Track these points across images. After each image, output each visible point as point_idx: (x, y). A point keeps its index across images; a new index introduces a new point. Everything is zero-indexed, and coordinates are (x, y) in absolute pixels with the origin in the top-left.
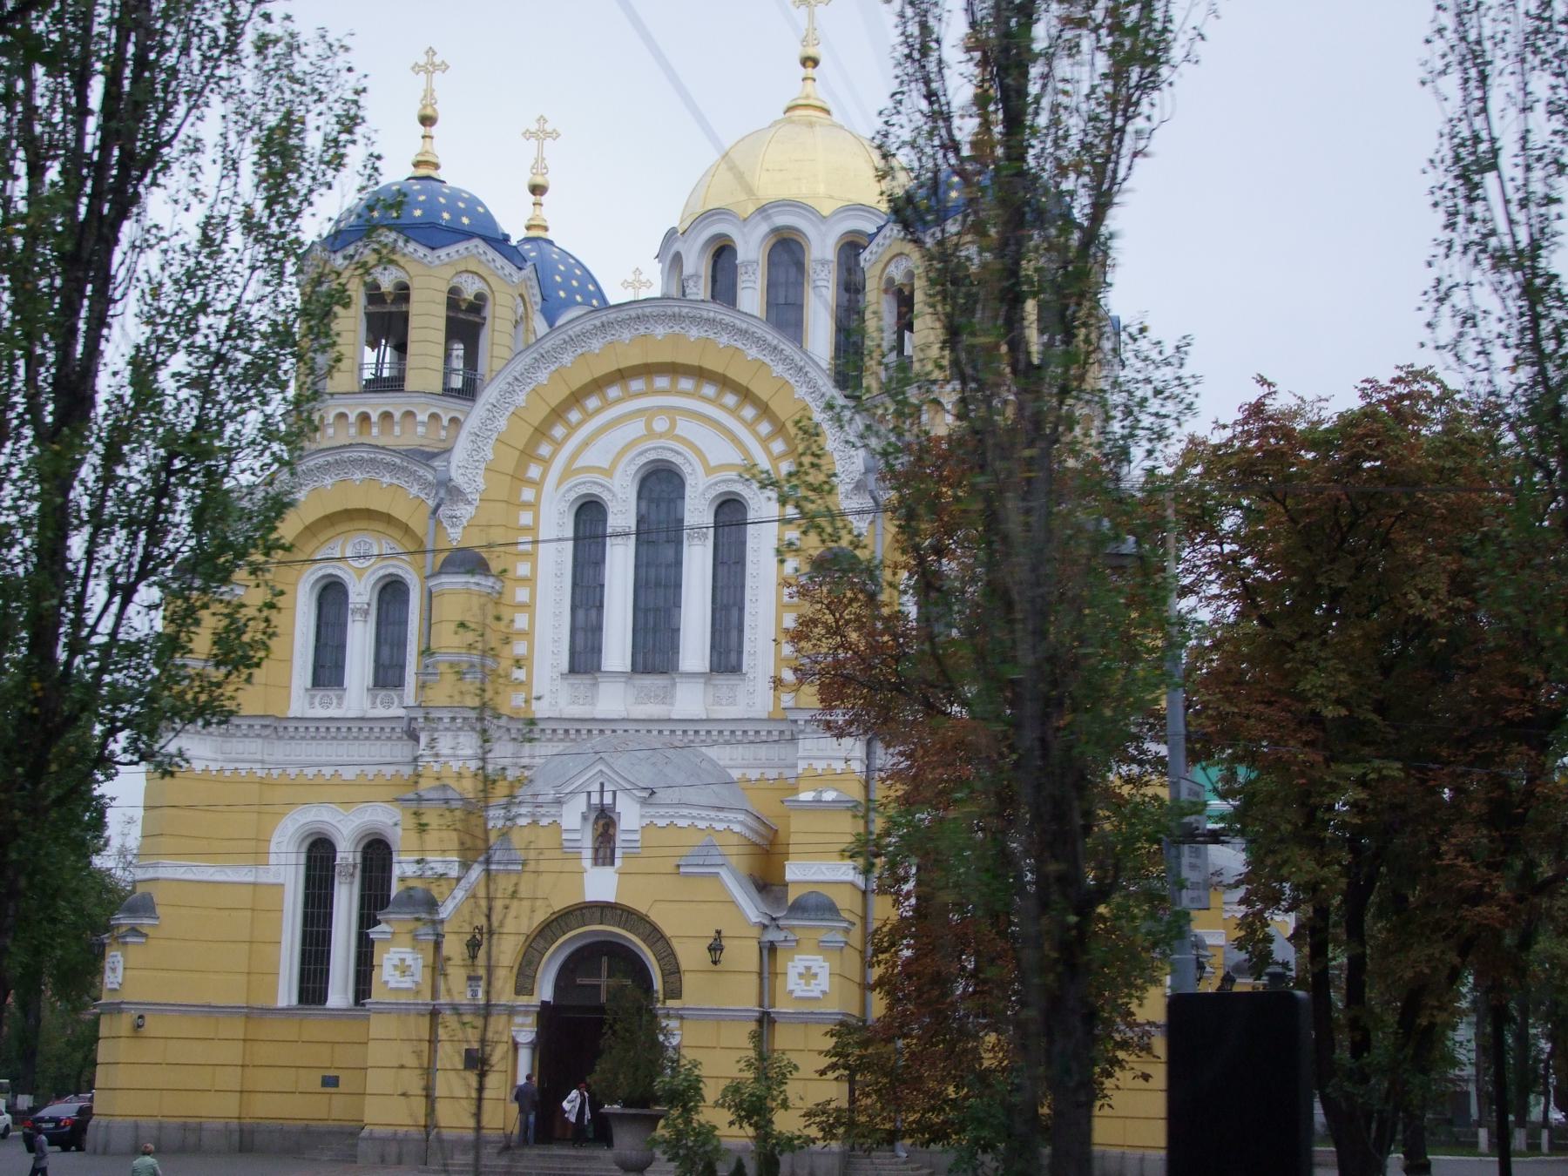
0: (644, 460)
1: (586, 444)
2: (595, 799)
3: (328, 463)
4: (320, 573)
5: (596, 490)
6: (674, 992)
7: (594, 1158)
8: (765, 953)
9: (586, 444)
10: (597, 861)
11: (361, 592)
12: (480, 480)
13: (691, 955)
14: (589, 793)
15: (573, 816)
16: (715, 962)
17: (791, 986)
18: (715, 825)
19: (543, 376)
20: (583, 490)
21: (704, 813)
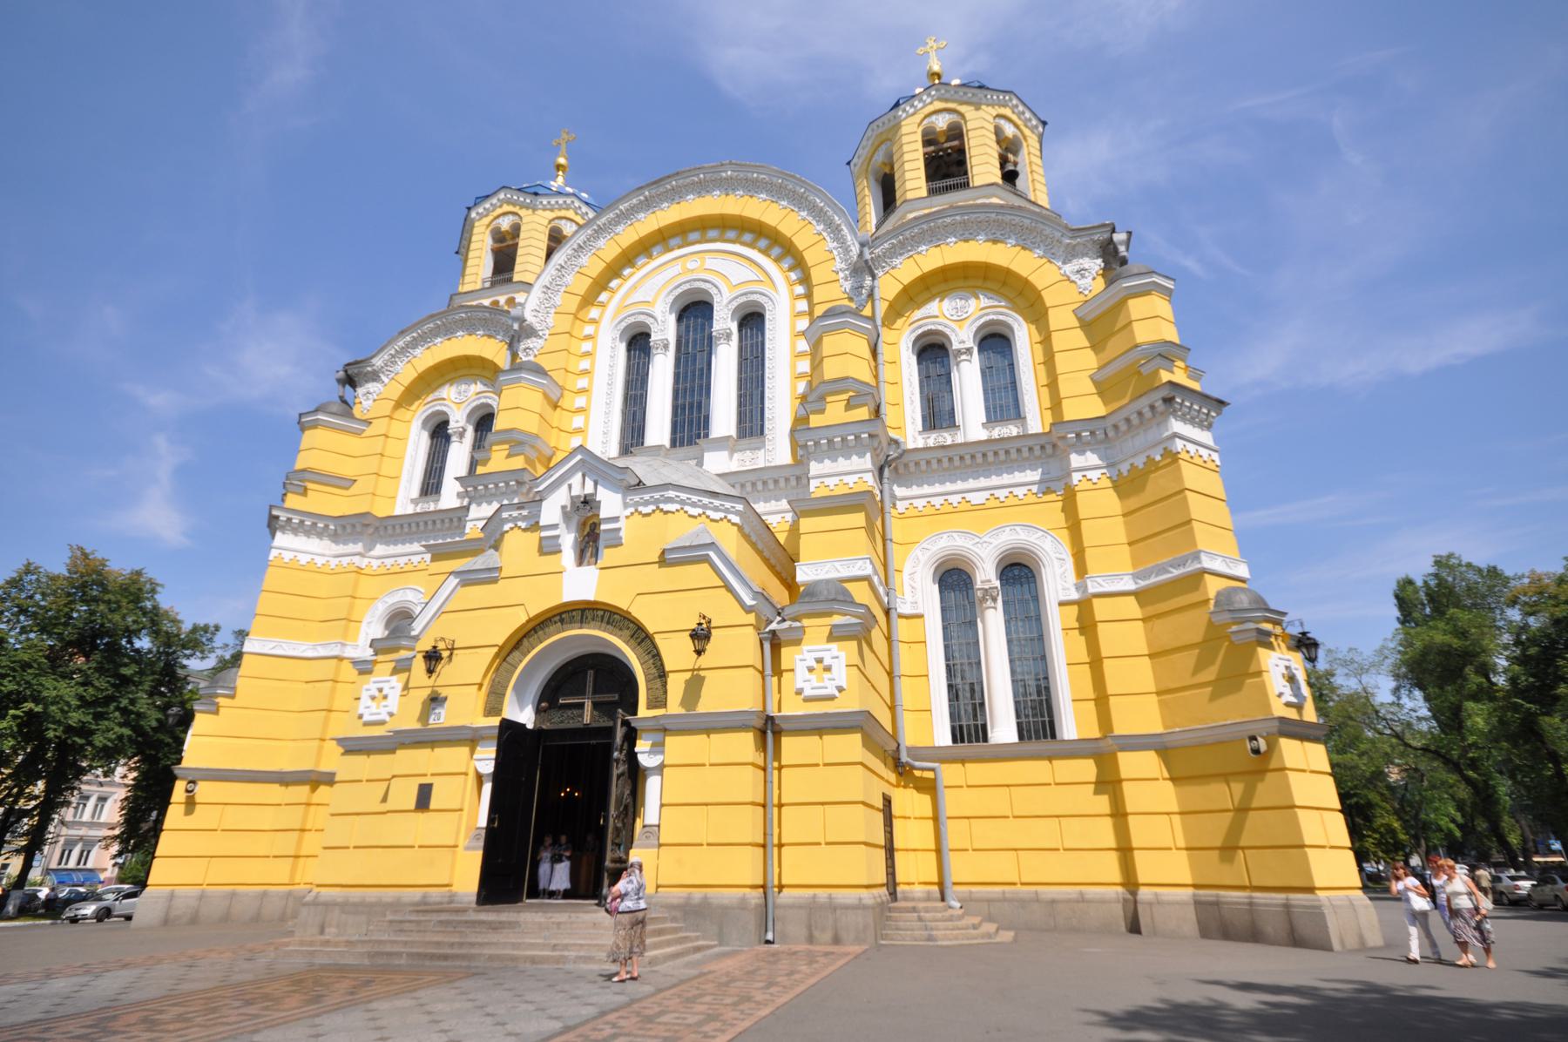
0: (679, 290)
1: (634, 287)
2: (575, 492)
3: (438, 327)
4: (430, 411)
5: (641, 318)
6: (658, 701)
7: (512, 925)
8: (767, 646)
9: (634, 287)
10: (581, 561)
11: (458, 419)
12: (550, 321)
13: (676, 653)
14: (570, 487)
15: (551, 511)
16: (699, 653)
17: (799, 685)
18: (709, 512)
19: (601, 243)
20: (632, 320)
21: (695, 498)
